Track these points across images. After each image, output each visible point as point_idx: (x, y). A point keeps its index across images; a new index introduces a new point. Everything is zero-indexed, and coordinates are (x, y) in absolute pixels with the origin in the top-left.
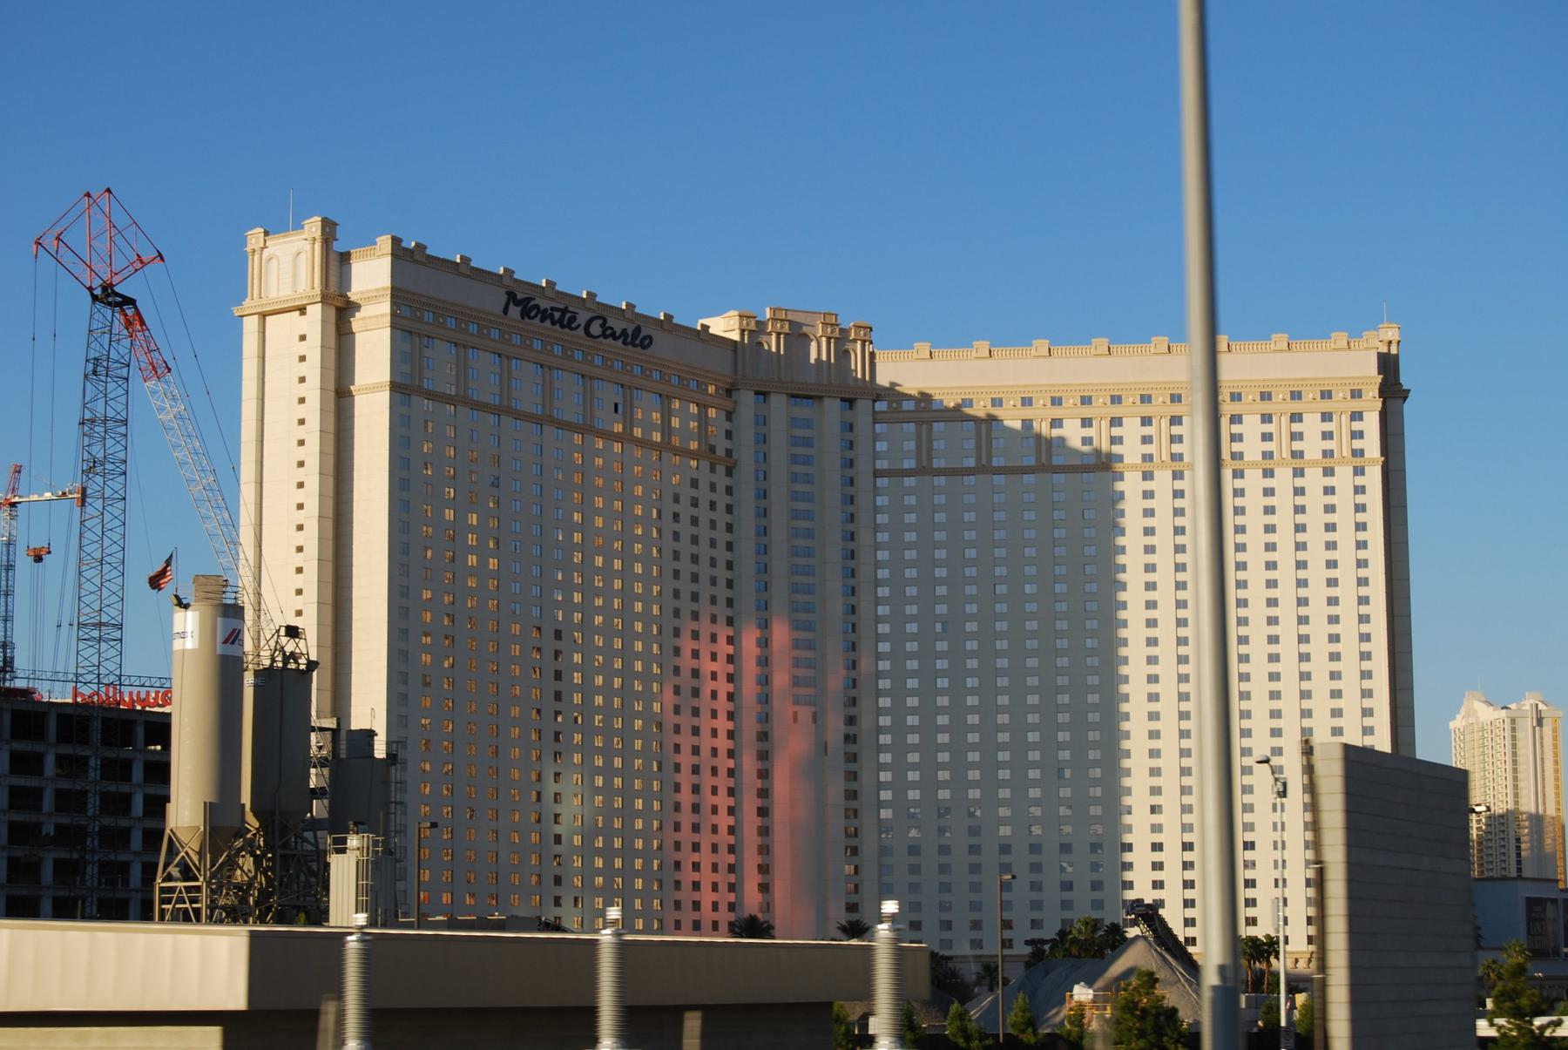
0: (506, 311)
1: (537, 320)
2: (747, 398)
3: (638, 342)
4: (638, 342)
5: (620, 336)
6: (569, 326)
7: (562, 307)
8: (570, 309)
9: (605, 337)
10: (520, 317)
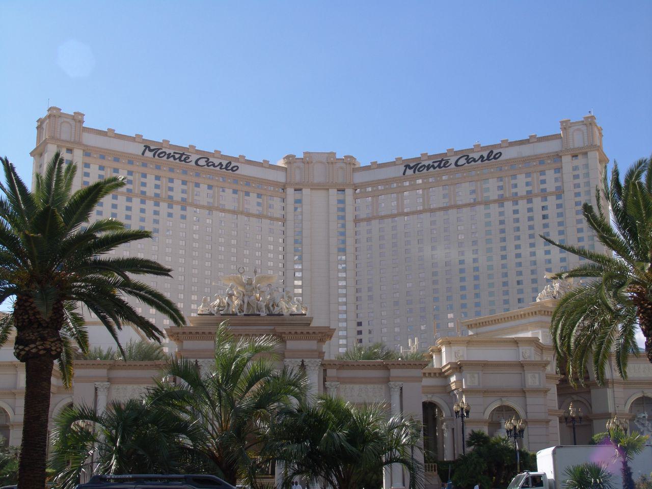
0: (143, 154)
1: (165, 158)
2: (290, 191)
3: (230, 168)
4: (230, 168)
5: (218, 166)
6: (185, 160)
7: (182, 153)
8: (185, 153)
9: (208, 166)
10: (152, 156)
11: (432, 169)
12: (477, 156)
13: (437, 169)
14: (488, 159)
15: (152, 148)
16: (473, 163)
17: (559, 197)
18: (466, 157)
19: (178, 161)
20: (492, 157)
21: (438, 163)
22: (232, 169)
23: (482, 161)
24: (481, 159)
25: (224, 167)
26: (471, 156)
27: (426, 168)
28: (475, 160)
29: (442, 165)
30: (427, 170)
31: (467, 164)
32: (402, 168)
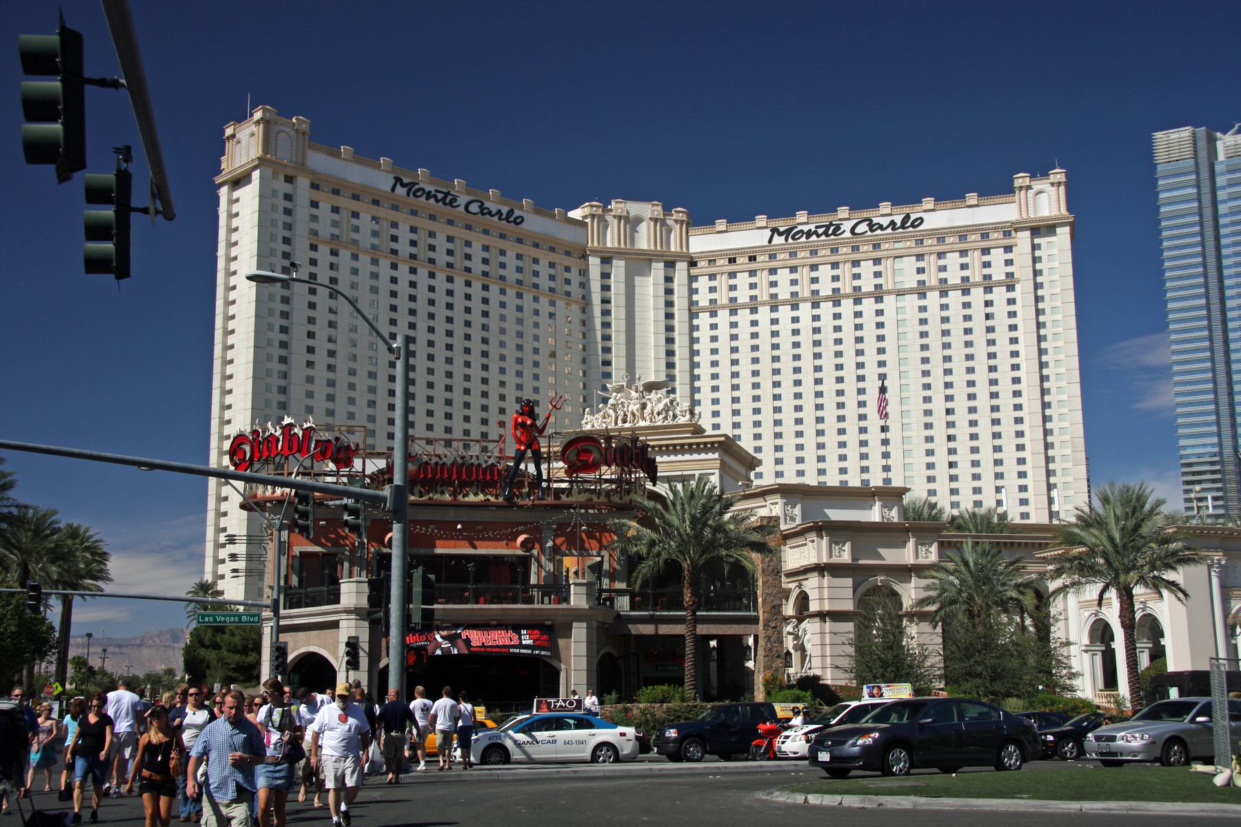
0: (393, 189)
1: (423, 199)
3: (512, 219)
4: (512, 219)
6: (451, 204)
9: (483, 214)
11: (814, 238)
12: (885, 221)
13: (823, 237)
14: (903, 226)
15: (406, 181)
16: (879, 232)
17: (1011, 288)
19: (441, 203)
20: (909, 224)
21: (823, 229)
22: (515, 222)
23: (893, 229)
25: (504, 216)
26: (875, 220)
28: (881, 227)
29: (830, 232)
30: (807, 238)
31: (869, 233)
32: (768, 233)
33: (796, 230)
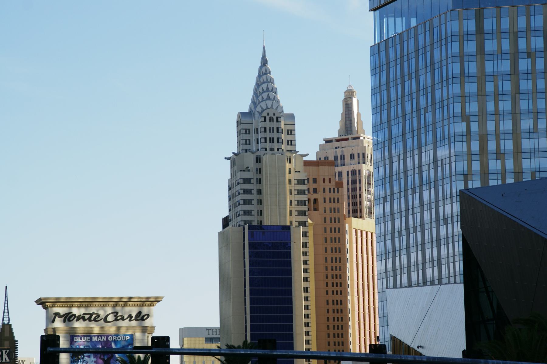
18: (115, 314)
21: (89, 316)
23: (130, 320)
24: (129, 318)
27: (76, 318)
29: (92, 319)
33: (71, 314)
